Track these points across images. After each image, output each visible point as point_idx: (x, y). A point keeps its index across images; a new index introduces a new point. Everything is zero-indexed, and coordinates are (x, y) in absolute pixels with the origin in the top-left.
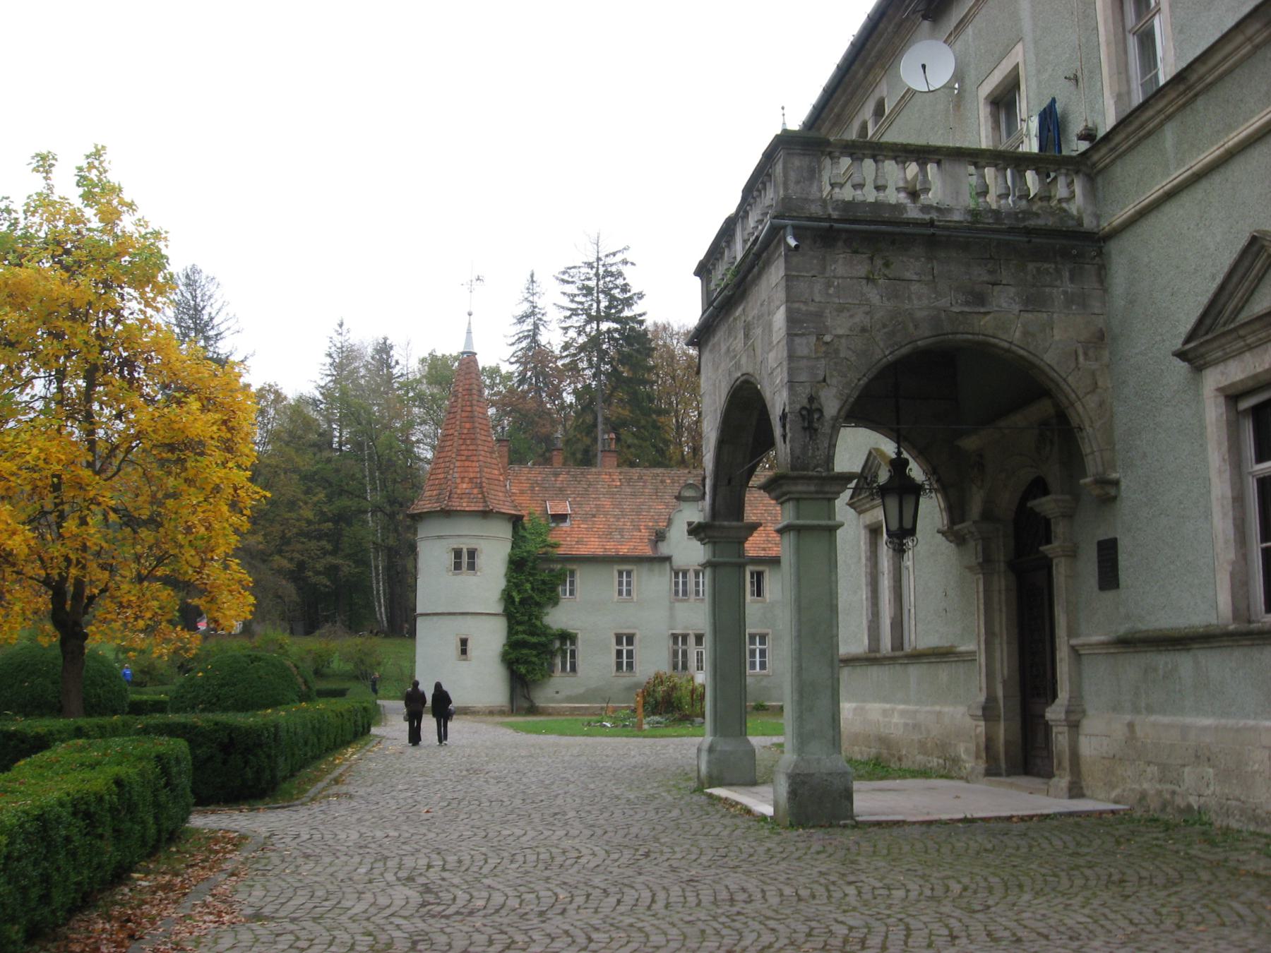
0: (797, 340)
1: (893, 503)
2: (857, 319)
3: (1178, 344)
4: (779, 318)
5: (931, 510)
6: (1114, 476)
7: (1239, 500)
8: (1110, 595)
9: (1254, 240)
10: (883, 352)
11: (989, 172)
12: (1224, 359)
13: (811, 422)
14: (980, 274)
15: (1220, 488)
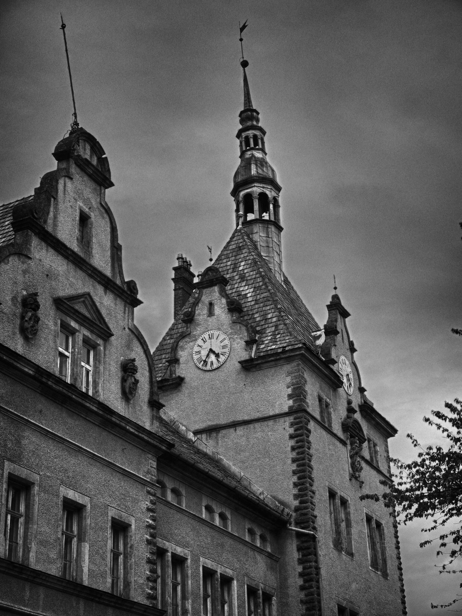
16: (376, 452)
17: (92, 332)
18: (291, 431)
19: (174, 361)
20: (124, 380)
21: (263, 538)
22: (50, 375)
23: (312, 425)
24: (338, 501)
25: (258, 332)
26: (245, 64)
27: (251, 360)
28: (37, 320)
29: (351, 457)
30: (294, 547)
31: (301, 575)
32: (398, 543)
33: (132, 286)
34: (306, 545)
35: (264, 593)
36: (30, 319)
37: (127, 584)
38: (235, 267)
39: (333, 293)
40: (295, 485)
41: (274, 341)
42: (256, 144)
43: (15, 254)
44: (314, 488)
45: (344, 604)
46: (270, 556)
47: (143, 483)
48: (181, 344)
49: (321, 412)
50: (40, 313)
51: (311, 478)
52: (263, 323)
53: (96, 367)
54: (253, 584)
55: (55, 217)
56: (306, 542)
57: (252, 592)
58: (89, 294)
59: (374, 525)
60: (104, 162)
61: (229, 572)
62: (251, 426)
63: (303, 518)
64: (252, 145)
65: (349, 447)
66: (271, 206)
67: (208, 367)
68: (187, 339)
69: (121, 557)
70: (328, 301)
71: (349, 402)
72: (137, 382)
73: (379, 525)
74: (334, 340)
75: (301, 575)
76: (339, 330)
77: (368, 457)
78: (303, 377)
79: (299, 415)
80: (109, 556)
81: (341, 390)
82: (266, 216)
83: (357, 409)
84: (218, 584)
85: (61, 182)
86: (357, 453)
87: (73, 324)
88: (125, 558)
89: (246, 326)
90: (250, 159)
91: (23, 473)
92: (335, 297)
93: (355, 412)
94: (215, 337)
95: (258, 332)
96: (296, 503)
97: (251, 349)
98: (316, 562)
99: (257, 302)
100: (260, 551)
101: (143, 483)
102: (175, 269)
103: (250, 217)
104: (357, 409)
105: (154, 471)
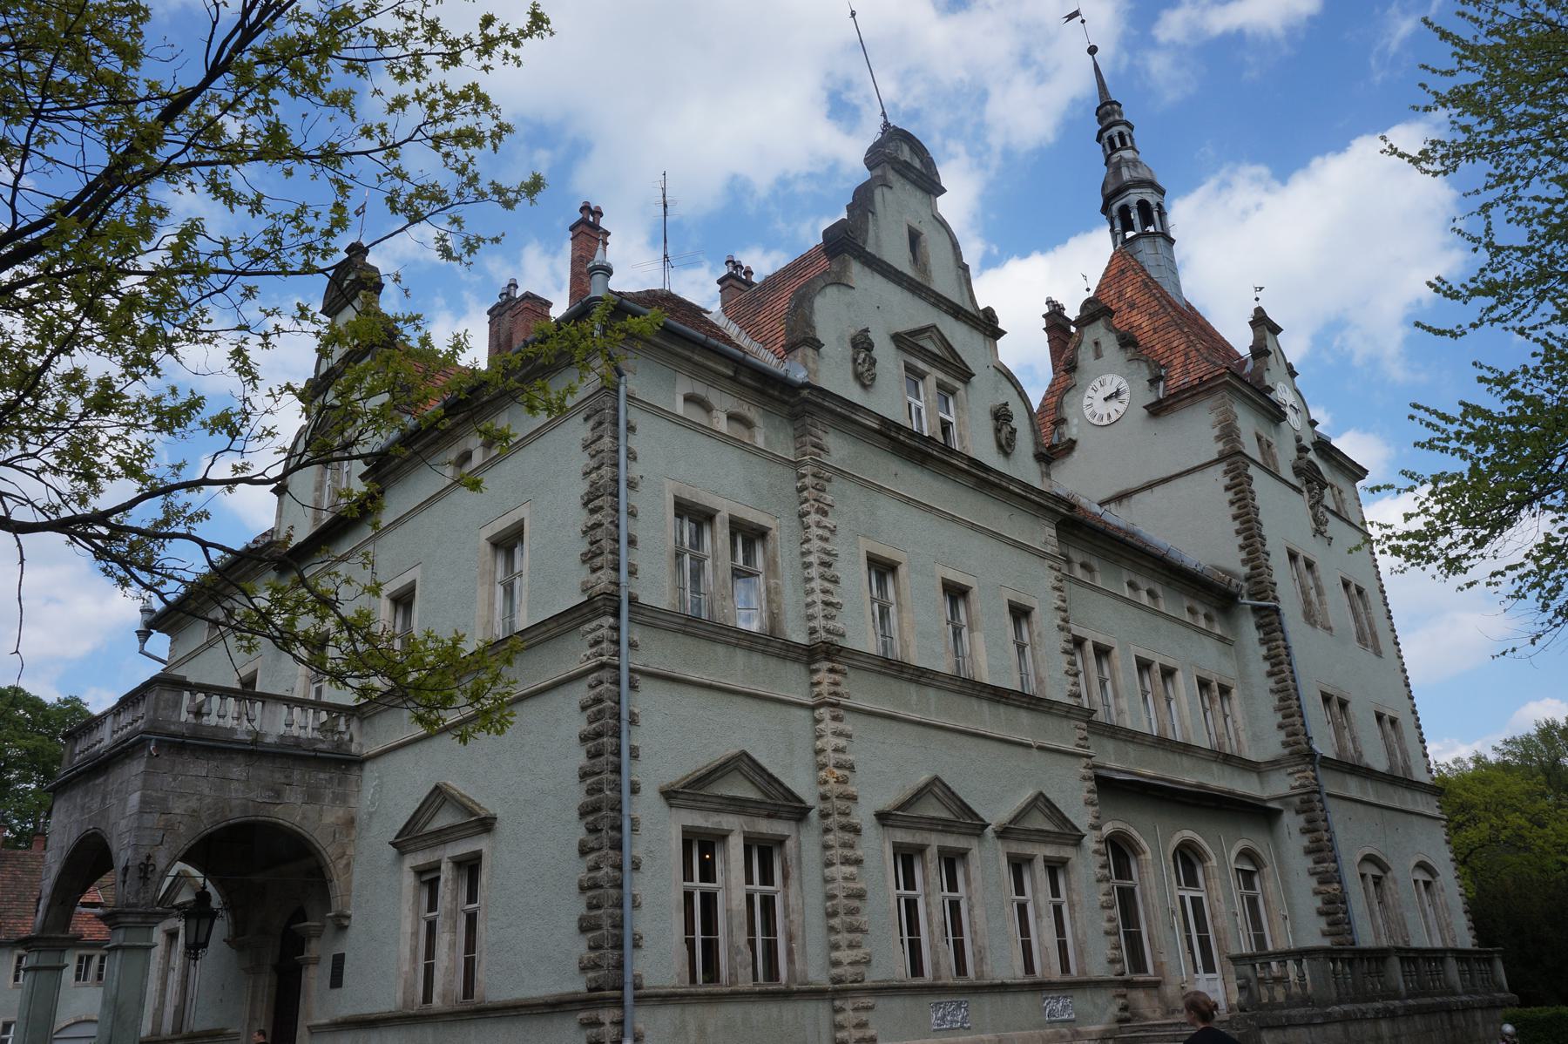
0: (146, 816)
1: (193, 923)
2: (190, 804)
3: (392, 837)
4: (135, 799)
5: (221, 928)
6: (349, 912)
7: (415, 934)
8: (336, 991)
9: (437, 787)
10: (205, 826)
11: (297, 711)
12: (416, 850)
13: (146, 873)
14: (279, 777)
15: (407, 926)
16: (1343, 501)
17: (947, 373)
18: (1227, 481)
19: (1060, 422)
20: (998, 430)
21: (1208, 618)
22: (899, 428)
23: (1253, 470)
24: (1302, 564)
25: (1163, 366)
27: (1160, 401)
28: (873, 362)
29: (1311, 507)
30: (1253, 627)
31: (1266, 658)
32: (1389, 611)
33: (989, 314)
34: (1267, 620)
35: (1220, 686)
36: (864, 360)
37: (1040, 681)
38: (1120, 295)
40: (1242, 548)
41: (1187, 373)
42: (1123, 142)
43: (831, 284)
44: (1267, 548)
45: (1329, 690)
46: (1221, 639)
47: (1043, 556)
48: (1066, 399)
49: (1263, 454)
50: (874, 353)
51: (1261, 536)
53: (958, 417)
54: (1204, 675)
55: (877, 237)
56: (1267, 616)
57: (1204, 685)
58: (935, 326)
59: (1353, 590)
60: (929, 163)
61: (1171, 663)
63: (1258, 587)
64: (1118, 145)
65: (1306, 495)
66: (1155, 214)
67: (1106, 422)
68: (1072, 392)
69: (1028, 649)
70: (1249, 314)
71: (1298, 440)
72: (1013, 431)
73: (1360, 591)
74: (1266, 363)
75: (1266, 658)
78: (1232, 412)
79: (1234, 459)
80: (1013, 649)
81: (1283, 424)
82: (1151, 229)
83: (1310, 446)
84: (1158, 677)
85: (878, 193)
86: (1318, 502)
87: (921, 365)
88: (1033, 649)
89: (1146, 361)
90: (1119, 161)
91: (885, 552)
93: (1306, 450)
94: (1108, 382)
95: (1163, 366)
96: (1246, 570)
97: (1158, 388)
98: (1284, 640)
99: (1155, 331)
100: (1208, 633)
102: (1044, 316)
103: (1129, 234)
104: (1310, 446)
105: (1054, 541)
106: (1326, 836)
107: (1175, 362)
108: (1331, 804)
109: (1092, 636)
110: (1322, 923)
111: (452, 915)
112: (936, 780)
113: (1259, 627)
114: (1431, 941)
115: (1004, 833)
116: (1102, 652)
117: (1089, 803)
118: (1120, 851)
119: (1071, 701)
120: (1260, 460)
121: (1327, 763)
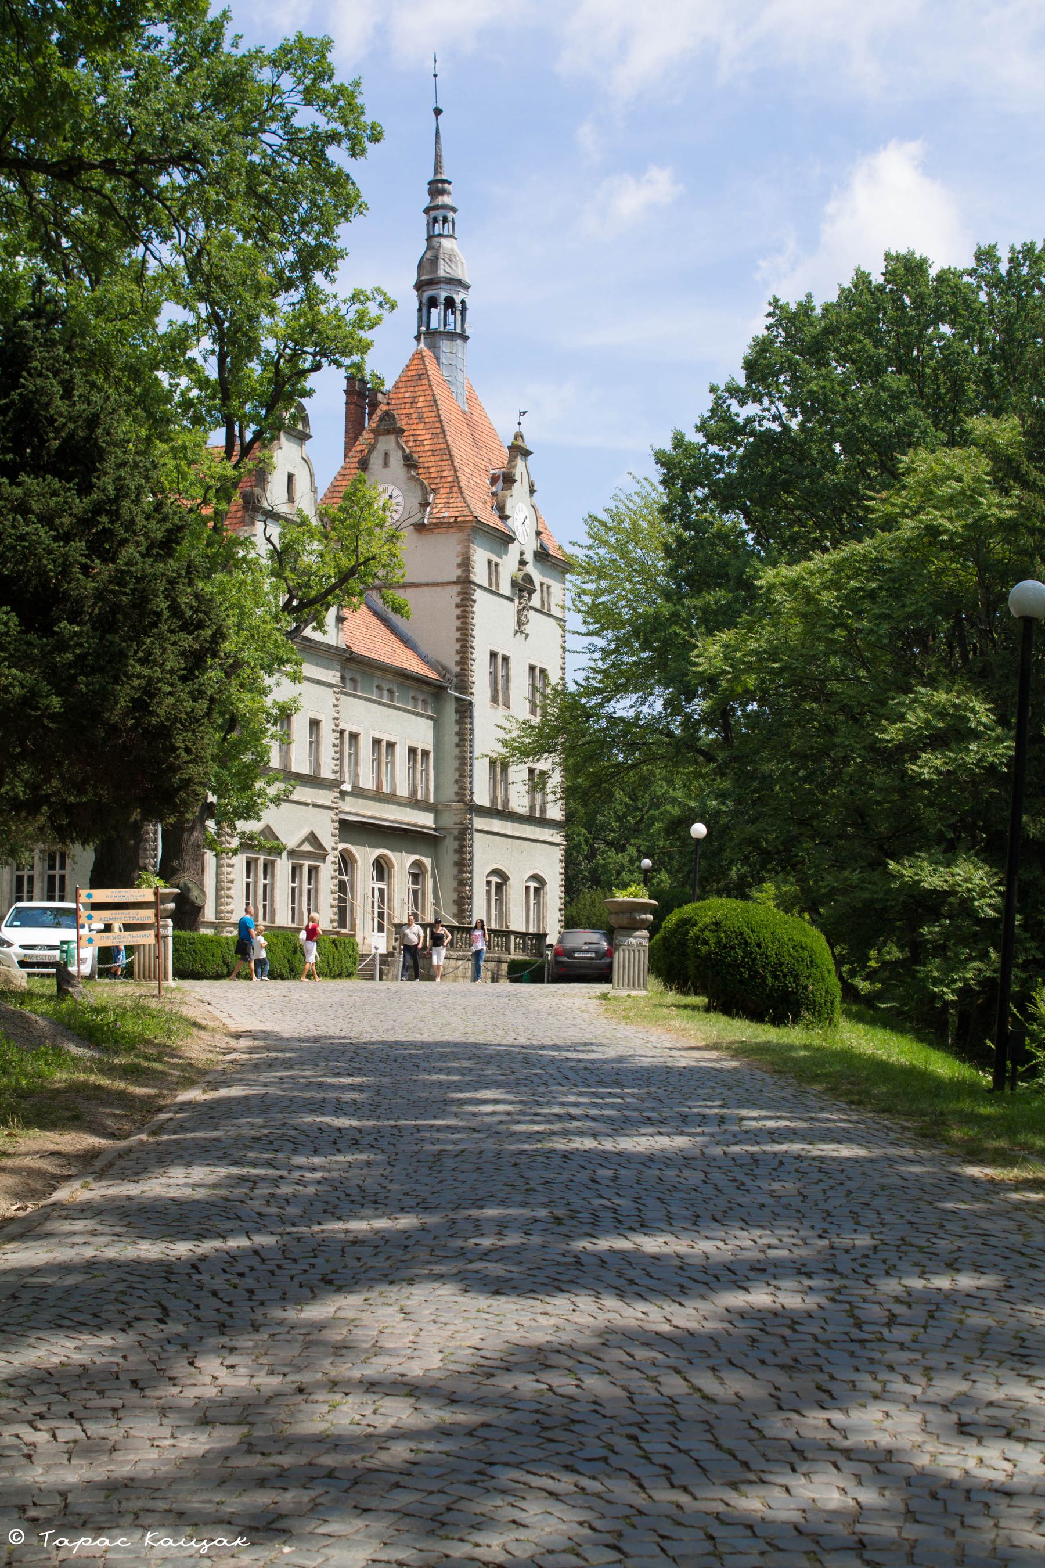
18: (458, 600)
23: (479, 595)
24: (499, 660)
26: (438, 112)
39: (516, 429)
40: (458, 652)
41: (447, 506)
47: (330, 685)
52: (438, 481)
54: (413, 745)
57: (412, 751)
61: (392, 739)
62: (421, 589)
65: (517, 601)
73: (543, 671)
76: (518, 477)
77: (538, 606)
92: (519, 436)
96: (456, 669)
101: (330, 685)
106: (468, 857)
107: (442, 491)
108: (476, 835)
109: (349, 727)
110: (455, 909)
111: (42, 874)
112: (268, 827)
113: (457, 711)
114: (527, 927)
115: (292, 854)
116: (354, 737)
117: (334, 835)
118: (346, 862)
119: (332, 777)
120: (486, 585)
121: (482, 812)
